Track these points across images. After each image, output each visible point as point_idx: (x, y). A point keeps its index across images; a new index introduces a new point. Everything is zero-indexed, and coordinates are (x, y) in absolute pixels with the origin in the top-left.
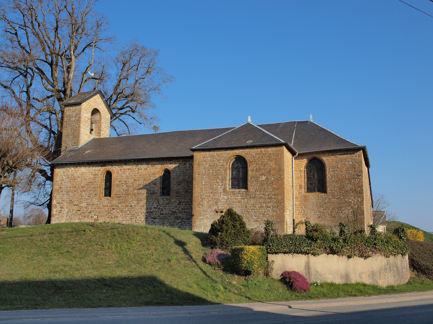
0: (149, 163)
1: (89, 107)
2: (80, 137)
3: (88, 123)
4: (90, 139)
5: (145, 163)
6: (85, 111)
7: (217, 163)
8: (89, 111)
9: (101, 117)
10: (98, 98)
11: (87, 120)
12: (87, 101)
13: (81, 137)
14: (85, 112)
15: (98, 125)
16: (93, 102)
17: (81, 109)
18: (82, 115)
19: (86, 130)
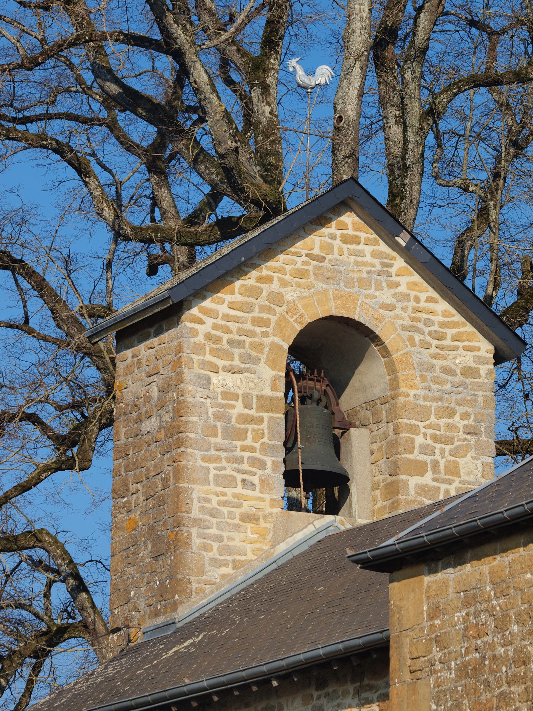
0: (371, 688)
1: (258, 322)
2: (188, 545)
3: (258, 435)
4: (282, 547)
5: (351, 688)
6: (215, 353)
7: (492, 646)
8: (258, 347)
9: (392, 369)
10: (346, 240)
11: (253, 412)
12: (238, 284)
13: (196, 541)
14: (220, 363)
15: (385, 436)
16: (302, 274)
17: (179, 349)
18: (189, 387)
19: (239, 489)
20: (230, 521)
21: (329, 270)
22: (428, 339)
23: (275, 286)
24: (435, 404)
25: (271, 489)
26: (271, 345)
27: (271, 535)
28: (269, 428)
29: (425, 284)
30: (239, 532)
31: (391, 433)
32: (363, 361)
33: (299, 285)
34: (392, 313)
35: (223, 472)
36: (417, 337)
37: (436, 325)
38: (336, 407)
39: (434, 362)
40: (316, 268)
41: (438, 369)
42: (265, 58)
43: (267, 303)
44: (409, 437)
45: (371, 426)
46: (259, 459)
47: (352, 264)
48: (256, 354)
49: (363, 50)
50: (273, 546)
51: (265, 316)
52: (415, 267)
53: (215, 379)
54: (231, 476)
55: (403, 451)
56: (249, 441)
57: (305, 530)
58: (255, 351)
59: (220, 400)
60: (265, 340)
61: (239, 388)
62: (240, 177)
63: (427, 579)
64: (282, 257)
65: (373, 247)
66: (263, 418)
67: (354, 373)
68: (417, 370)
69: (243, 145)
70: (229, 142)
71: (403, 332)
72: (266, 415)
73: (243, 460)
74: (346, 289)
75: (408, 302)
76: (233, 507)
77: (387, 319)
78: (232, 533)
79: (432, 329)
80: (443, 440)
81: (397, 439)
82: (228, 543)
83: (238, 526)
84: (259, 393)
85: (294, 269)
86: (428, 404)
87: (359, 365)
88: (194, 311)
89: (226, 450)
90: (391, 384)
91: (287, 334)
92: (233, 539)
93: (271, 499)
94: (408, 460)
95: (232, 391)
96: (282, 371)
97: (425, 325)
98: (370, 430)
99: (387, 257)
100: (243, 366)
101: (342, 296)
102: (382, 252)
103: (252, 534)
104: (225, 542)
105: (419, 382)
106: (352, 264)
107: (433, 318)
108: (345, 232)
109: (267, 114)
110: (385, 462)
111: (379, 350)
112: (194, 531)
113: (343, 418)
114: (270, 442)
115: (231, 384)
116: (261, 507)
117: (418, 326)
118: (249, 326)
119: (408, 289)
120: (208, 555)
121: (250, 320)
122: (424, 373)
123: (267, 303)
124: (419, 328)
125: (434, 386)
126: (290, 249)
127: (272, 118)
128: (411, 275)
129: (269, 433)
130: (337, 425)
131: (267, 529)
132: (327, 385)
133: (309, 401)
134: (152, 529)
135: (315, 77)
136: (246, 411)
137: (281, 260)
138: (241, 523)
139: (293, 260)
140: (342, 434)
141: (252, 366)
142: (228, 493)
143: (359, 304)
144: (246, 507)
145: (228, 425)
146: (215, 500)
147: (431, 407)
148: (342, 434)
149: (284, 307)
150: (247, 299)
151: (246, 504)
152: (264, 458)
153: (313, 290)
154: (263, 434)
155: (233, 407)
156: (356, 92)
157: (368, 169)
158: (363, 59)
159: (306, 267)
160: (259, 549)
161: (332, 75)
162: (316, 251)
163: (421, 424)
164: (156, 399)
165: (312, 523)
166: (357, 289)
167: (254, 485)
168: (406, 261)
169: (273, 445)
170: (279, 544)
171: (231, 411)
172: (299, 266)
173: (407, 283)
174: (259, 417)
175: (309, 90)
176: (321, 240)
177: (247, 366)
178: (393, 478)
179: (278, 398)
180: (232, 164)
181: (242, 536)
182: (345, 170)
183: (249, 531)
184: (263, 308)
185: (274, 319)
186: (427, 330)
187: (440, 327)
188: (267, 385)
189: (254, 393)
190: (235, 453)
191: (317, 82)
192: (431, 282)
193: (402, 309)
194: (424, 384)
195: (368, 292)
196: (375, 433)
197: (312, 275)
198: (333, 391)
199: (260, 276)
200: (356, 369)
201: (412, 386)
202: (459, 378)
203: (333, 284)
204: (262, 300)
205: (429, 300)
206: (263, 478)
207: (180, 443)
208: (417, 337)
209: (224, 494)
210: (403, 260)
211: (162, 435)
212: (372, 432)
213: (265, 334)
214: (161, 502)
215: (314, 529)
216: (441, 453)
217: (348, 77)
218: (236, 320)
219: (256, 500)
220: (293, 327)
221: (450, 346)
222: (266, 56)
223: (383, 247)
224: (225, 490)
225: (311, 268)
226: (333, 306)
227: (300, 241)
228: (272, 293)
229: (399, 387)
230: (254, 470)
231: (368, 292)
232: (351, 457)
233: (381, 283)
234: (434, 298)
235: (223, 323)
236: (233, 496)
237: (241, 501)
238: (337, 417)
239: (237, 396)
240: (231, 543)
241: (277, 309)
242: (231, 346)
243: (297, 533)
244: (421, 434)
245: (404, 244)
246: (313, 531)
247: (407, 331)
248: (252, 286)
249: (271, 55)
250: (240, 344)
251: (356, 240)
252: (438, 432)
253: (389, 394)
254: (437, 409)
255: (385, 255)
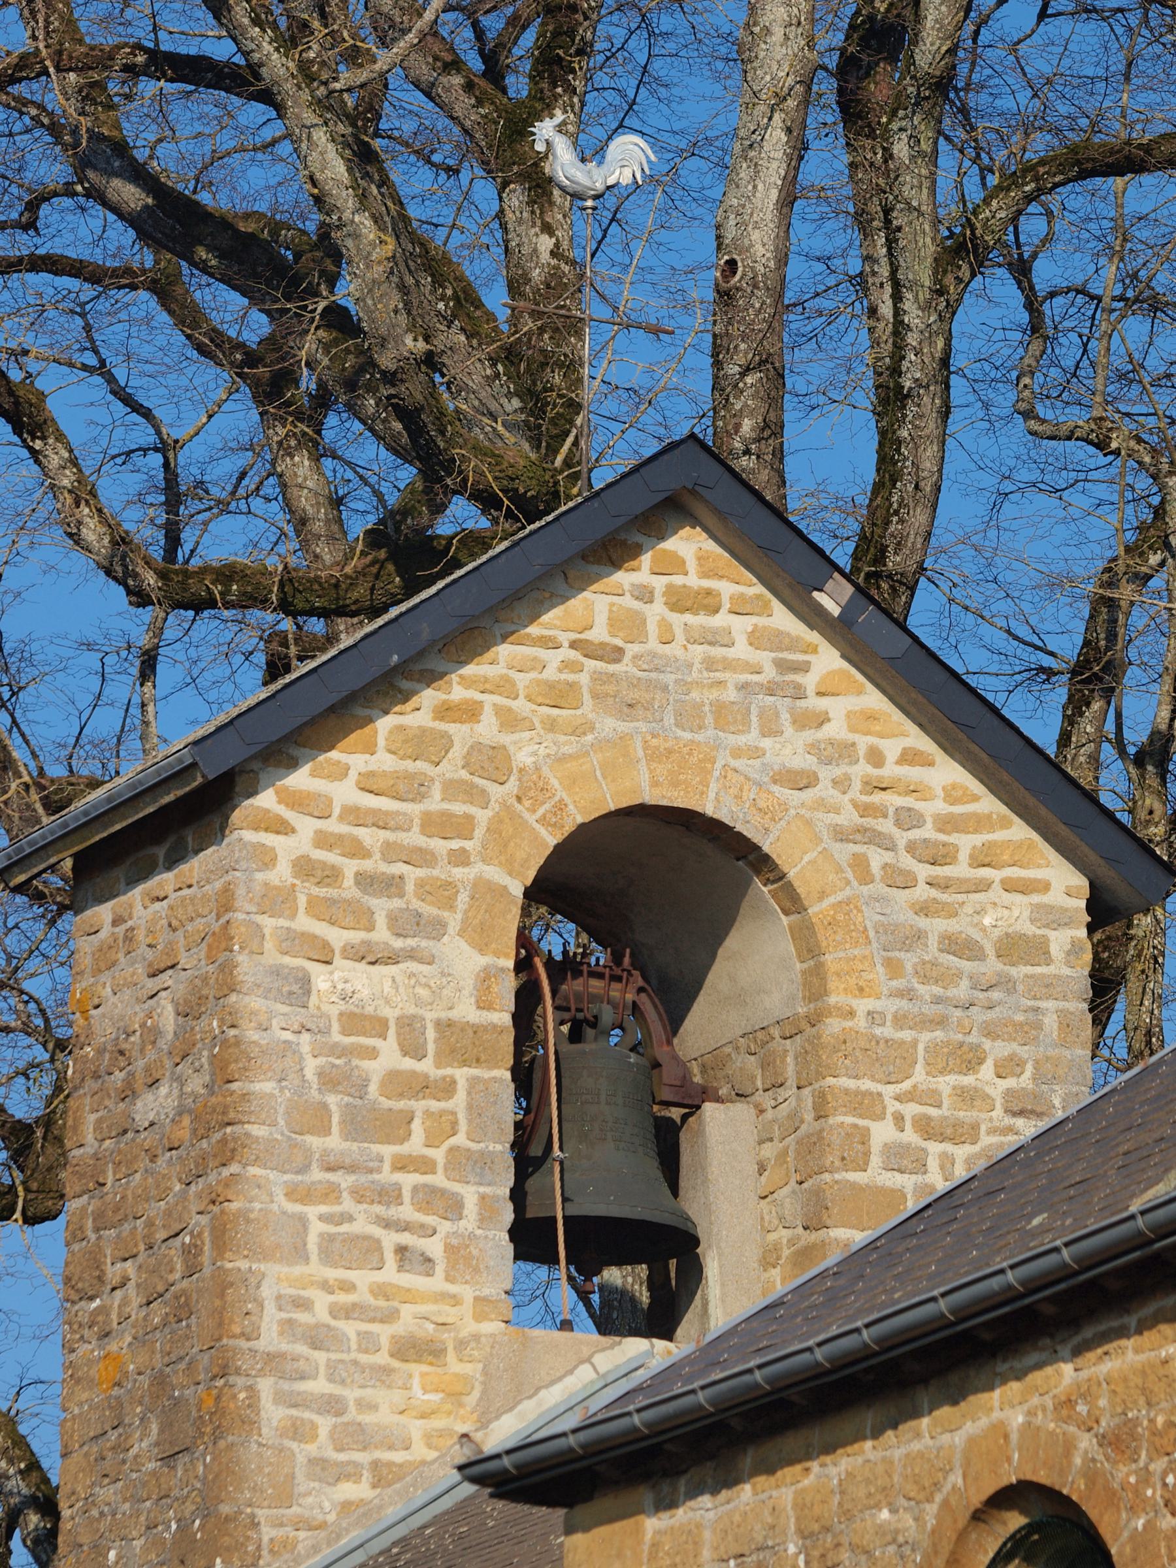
2: (249, 1422)
6: (322, 909)
8: (443, 893)
10: (680, 601)
11: (426, 1066)
12: (385, 724)
13: (272, 1414)
14: (337, 937)
15: (794, 1122)
17: (225, 903)
18: (252, 1003)
19: (390, 1273)
20: (364, 1358)
21: (635, 684)
22: (907, 862)
23: (487, 729)
24: (925, 1037)
25: (477, 1270)
26: (475, 885)
27: (476, 1394)
28: (470, 1107)
29: (897, 715)
30: (389, 1387)
31: (809, 1116)
32: (737, 924)
33: (551, 726)
34: (808, 795)
35: (345, 1228)
36: (877, 859)
37: (929, 825)
38: (666, 1048)
39: (922, 922)
40: (597, 677)
41: (933, 942)
42: (539, 106)
43: (464, 774)
44: (855, 1126)
45: (759, 1097)
46: (443, 1192)
47: (697, 666)
48: (434, 911)
49: (790, 81)
50: (484, 1425)
51: (458, 808)
52: (870, 671)
53: (322, 979)
54: (367, 1238)
55: (837, 1163)
56: (415, 1144)
57: (570, 1381)
58: (432, 903)
59: (336, 1037)
60: (458, 872)
61: (387, 1001)
62: (442, 432)
63: (652, 1524)
64: (504, 651)
65: (754, 619)
66: (454, 1082)
67: (713, 957)
68: (875, 945)
69: (475, 342)
70: (409, 340)
71: (838, 845)
72: (461, 1075)
73: (400, 1196)
74: (679, 733)
75: (850, 763)
76: (373, 1320)
77: (792, 812)
78: (369, 1391)
79: (915, 834)
80: (949, 1131)
81: (822, 1130)
82: (360, 1418)
83: (387, 1371)
84: (443, 1015)
85: (538, 682)
86: (906, 1035)
87: (727, 934)
88: (266, 800)
89: (352, 1169)
90: (806, 984)
91: (520, 855)
92: (373, 1407)
93: (476, 1299)
94: (853, 1186)
95: (369, 1010)
96: (506, 956)
97: (898, 823)
98: (756, 1106)
99: (794, 644)
100: (398, 943)
101: (670, 751)
102: (779, 633)
103: (425, 1391)
104: (352, 1414)
105: (883, 978)
106: (697, 666)
107: (919, 806)
108: (678, 580)
109: (545, 257)
110: (794, 1192)
111: (774, 894)
112: (265, 1386)
113: (686, 1077)
114: (474, 1146)
115: (365, 993)
116: (449, 1320)
117: (879, 828)
118: (414, 838)
119: (852, 729)
120: (302, 1451)
121: (417, 821)
122: (897, 954)
123: (464, 774)
124: (880, 833)
125: (922, 989)
126: (529, 630)
127: (557, 268)
128: (860, 692)
129: (470, 1121)
130: (666, 1094)
131: (465, 1379)
132: (641, 990)
133: (589, 1032)
134: (161, 1381)
135: (604, 167)
136: (408, 1064)
137: (501, 659)
138: (396, 1364)
139: (535, 659)
140: (685, 1118)
141: (424, 943)
142: (358, 1283)
143: (716, 774)
144: (408, 1320)
145: (359, 1102)
146: (322, 1302)
147: (915, 1043)
148: (685, 1118)
149: (512, 785)
150: (410, 765)
151: (407, 1311)
152: (456, 1187)
153: (589, 738)
154: (454, 1124)
155: (373, 1054)
156: (774, 194)
157: (822, 399)
158: (791, 103)
159: (571, 677)
160: (441, 1433)
161: (649, 162)
162: (599, 633)
163: (889, 1091)
164: (170, 1036)
165: (588, 1360)
166: (711, 732)
167: (429, 1260)
168: (843, 656)
169: (482, 1153)
170: (497, 1417)
171: (366, 1064)
172: (550, 674)
173: (849, 715)
174: (444, 1078)
175: (589, 203)
176: (612, 604)
177: (411, 942)
178: (813, 1237)
179: (495, 1026)
180: (419, 397)
181: (397, 1396)
182: (746, 405)
183: (416, 1383)
184: (453, 789)
185: (483, 816)
186: (902, 838)
187: (940, 830)
188: (466, 992)
189: (430, 1016)
190: (376, 1177)
191: (611, 182)
192: (913, 711)
193: (835, 782)
194: (894, 983)
195: (742, 740)
196: (770, 1115)
197: (587, 697)
198: (656, 1007)
199: (445, 702)
200: (720, 944)
201: (861, 989)
202: (992, 965)
203: (645, 719)
204: (452, 768)
205: (909, 757)
206: (455, 1242)
207: (227, 1153)
208: (877, 859)
209: (348, 1287)
210: (837, 654)
211: (183, 1132)
212: (762, 1111)
213: (460, 858)
214: (182, 1310)
215: (594, 1376)
216: (942, 1167)
217: (752, 154)
218: (380, 821)
219: (436, 1302)
220: (536, 837)
221: (967, 880)
222: (542, 99)
223: (782, 619)
224: (352, 1275)
225: (584, 679)
226: (644, 778)
227: (553, 606)
228: (476, 747)
229: (826, 993)
230: (430, 1220)
231: (742, 740)
232: (706, 1181)
233: (777, 714)
234: (922, 753)
235: (344, 829)
236: (372, 1292)
237: (395, 1304)
238: (669, 1074)
239: (384, 1023)
240: (367, 1418)
241: (494, 790)
242: (365, 892)
243: (547, 1387)
244: (889, 1117)
245: (835, 610)
246: (592, 1382)
247: (848, 841)
248: (423, 731)
249: (556, 97)
250: (391, 886)
251: (707, 603)
252: (933, 1112)
253: (802, 1010)
254: (933, 1050)
255: (787, 641)
